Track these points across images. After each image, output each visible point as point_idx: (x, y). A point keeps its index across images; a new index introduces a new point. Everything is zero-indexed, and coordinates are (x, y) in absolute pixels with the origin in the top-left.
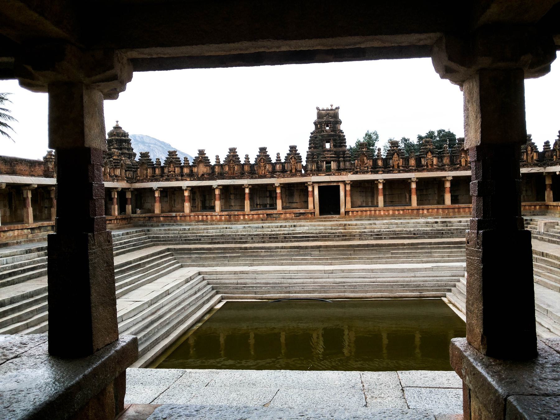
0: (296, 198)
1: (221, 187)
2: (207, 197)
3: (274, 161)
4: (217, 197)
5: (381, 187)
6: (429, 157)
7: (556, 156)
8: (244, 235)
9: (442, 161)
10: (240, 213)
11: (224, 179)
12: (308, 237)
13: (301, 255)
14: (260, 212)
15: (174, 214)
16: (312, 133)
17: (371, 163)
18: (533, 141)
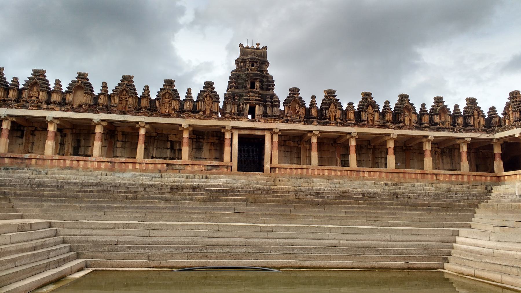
0: (205, 152)
1: (105, 124)
2: (83, 142)
3: (182, 97)
4: (98, 136)
5: (315, 140)
6: (370, 111)
7: (509, 120)
8: (133, 185)
9: (384, 117)
10: (128, 160)
11: (110, 113)
12: (226, 191)
13: (220, 209)
14: (157, 161)
15: (27, 156)
16: (233, 71)
17: (304, 112)
18: (478, 105)
